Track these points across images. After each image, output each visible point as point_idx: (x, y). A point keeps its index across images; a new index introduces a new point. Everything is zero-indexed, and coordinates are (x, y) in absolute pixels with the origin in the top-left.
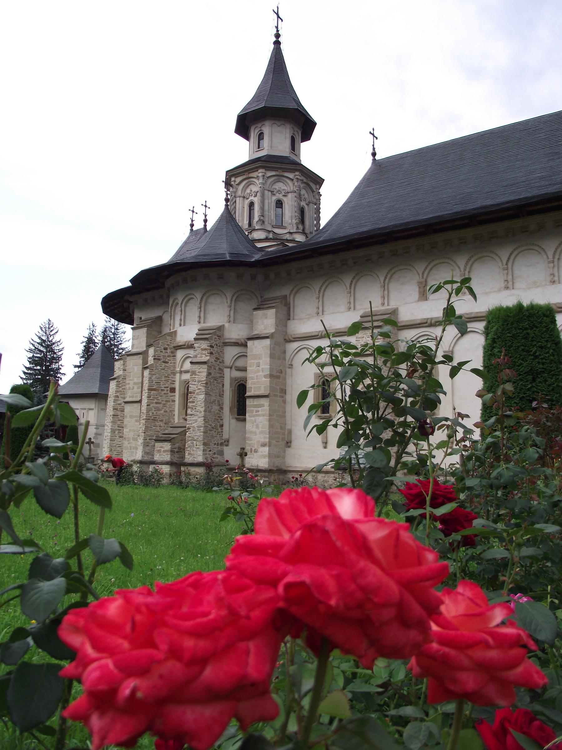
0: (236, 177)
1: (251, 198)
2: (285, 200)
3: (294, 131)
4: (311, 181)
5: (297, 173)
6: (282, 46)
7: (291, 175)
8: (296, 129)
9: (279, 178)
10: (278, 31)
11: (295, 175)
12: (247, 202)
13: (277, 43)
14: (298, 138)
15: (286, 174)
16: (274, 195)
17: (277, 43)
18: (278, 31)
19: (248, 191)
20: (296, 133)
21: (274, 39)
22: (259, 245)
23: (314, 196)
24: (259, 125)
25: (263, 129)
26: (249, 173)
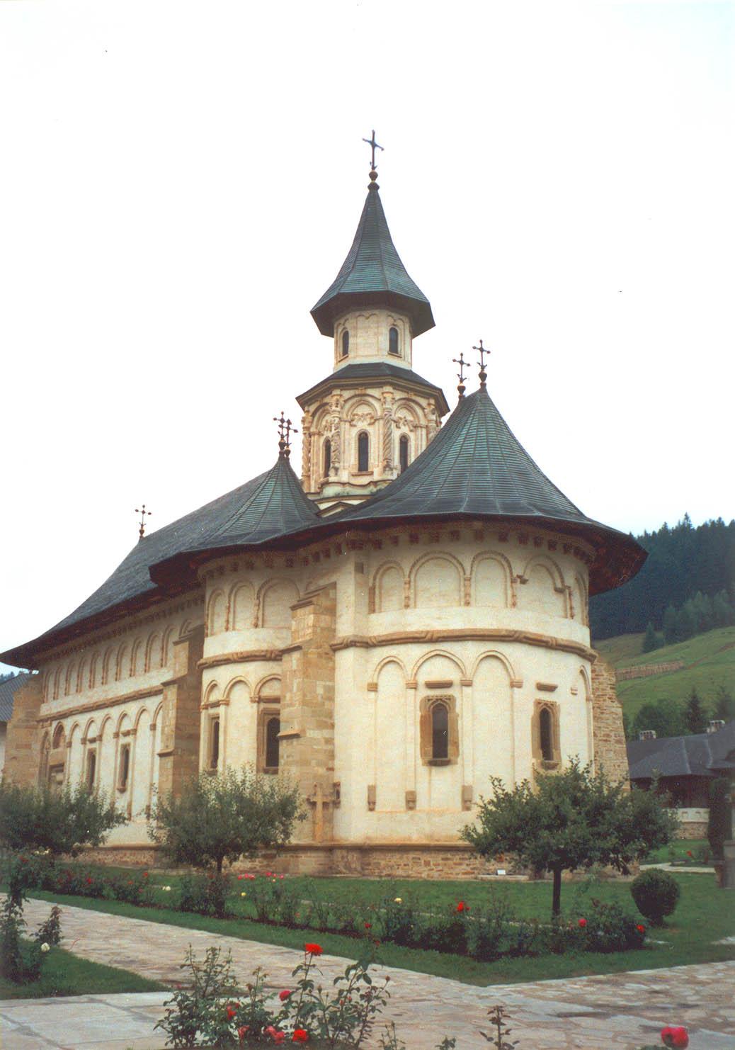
0: (310, 405)
1: (328, 434)
2: (371, 430)
3: (395, 321)
4: (415, 395)
5: (388, 389)
6: (380, 192)
7: (375, 392)
8: (396, 316)
9: (362, 399)
10: (374, 168)
11: (383, 393)
12: (322, 440)
13: (374, 188)
14: (404, 329)
15: (370, 391)
16: (355, 426)
17: (374, 188)
18: (374, 168)
19: (324, 423)
20: (399, 323)
21: (369, 181)
22: (323, 506)
23: (425, 415)
24: (342, 321)
25: (347, 325)
26: (323, 398)
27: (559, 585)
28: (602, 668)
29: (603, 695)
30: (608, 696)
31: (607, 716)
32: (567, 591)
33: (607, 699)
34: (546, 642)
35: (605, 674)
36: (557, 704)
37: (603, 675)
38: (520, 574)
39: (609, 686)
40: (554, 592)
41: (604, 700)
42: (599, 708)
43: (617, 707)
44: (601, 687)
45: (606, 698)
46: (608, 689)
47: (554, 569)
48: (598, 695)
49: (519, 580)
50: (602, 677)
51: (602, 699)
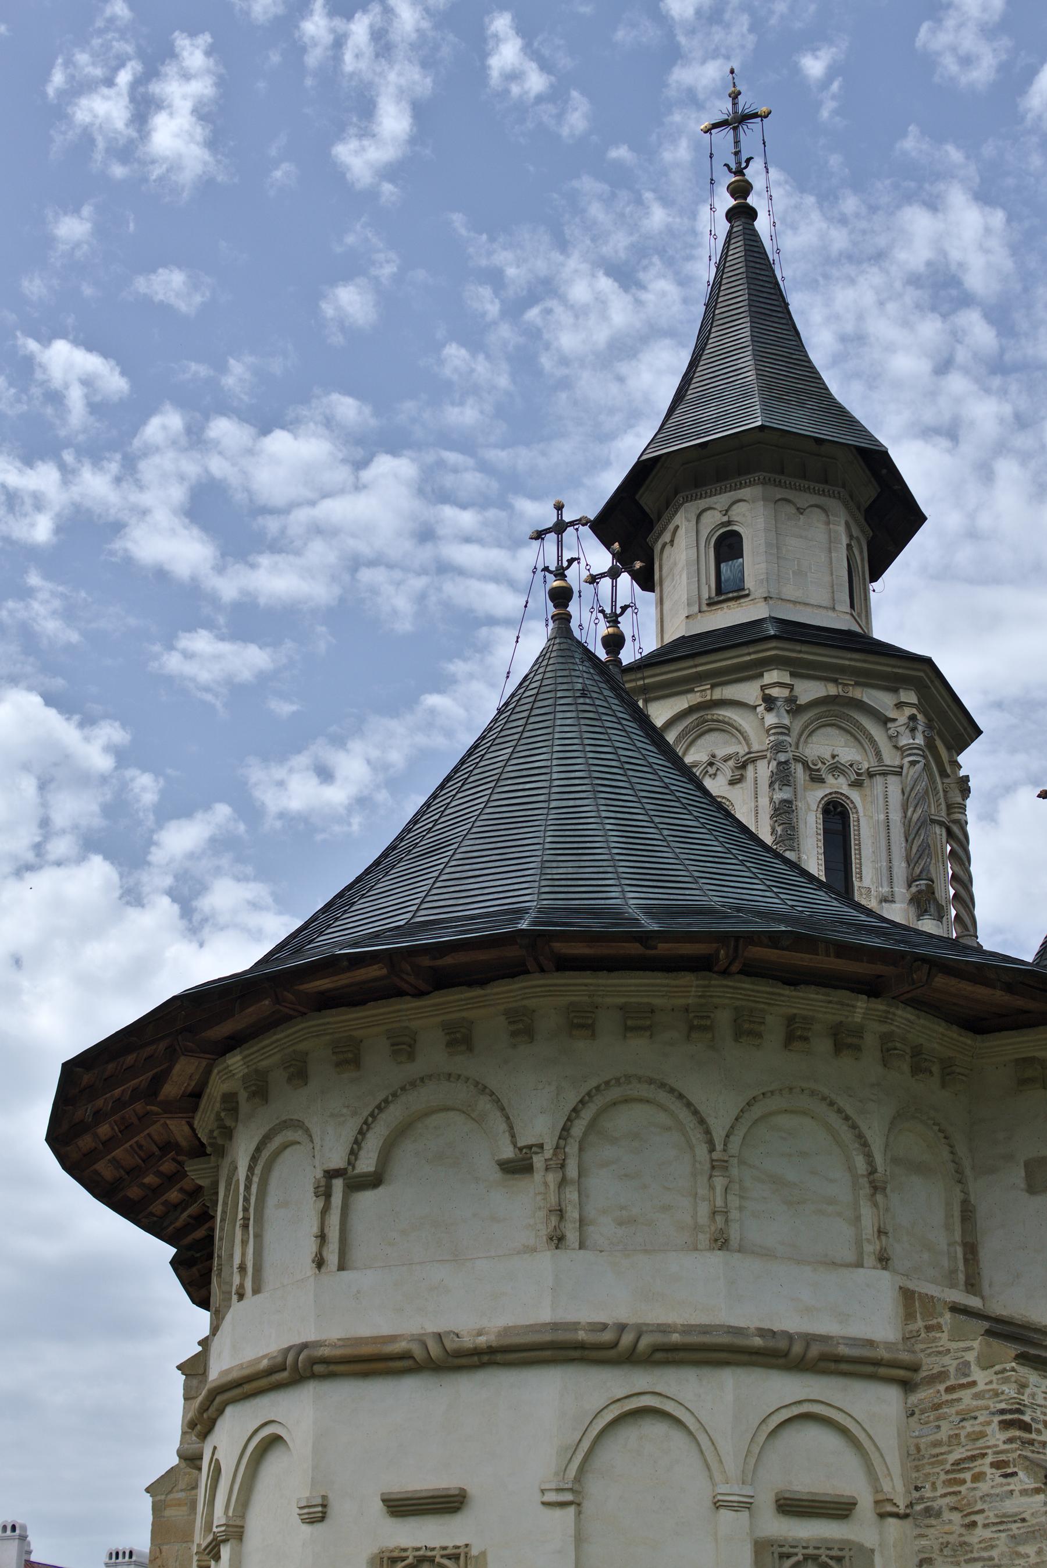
27: (508, 1152)
28: (971, 1357)
29: (973, 1458)
30: (989, 1459)
31: (987, 1534)
32: (538, 1161)
33: (989, 1471)
34: (406, 1356)
35: (980, 1376)
36: (474, 1552)
37: (974, 1383)
38: (337, 1159)
39: (997, 1419)
40: (496, 1174)
41: (978, 1477)
42: (956, 1509)
43: (1024, 1492)
44: (969, 1427)
45: (984, 1465)
46: (995, 1425)
47: (484, 1104)
48: (956, 1463)
49: (338, 1184)
50: (966, 1395)
51: (967, 1476)
